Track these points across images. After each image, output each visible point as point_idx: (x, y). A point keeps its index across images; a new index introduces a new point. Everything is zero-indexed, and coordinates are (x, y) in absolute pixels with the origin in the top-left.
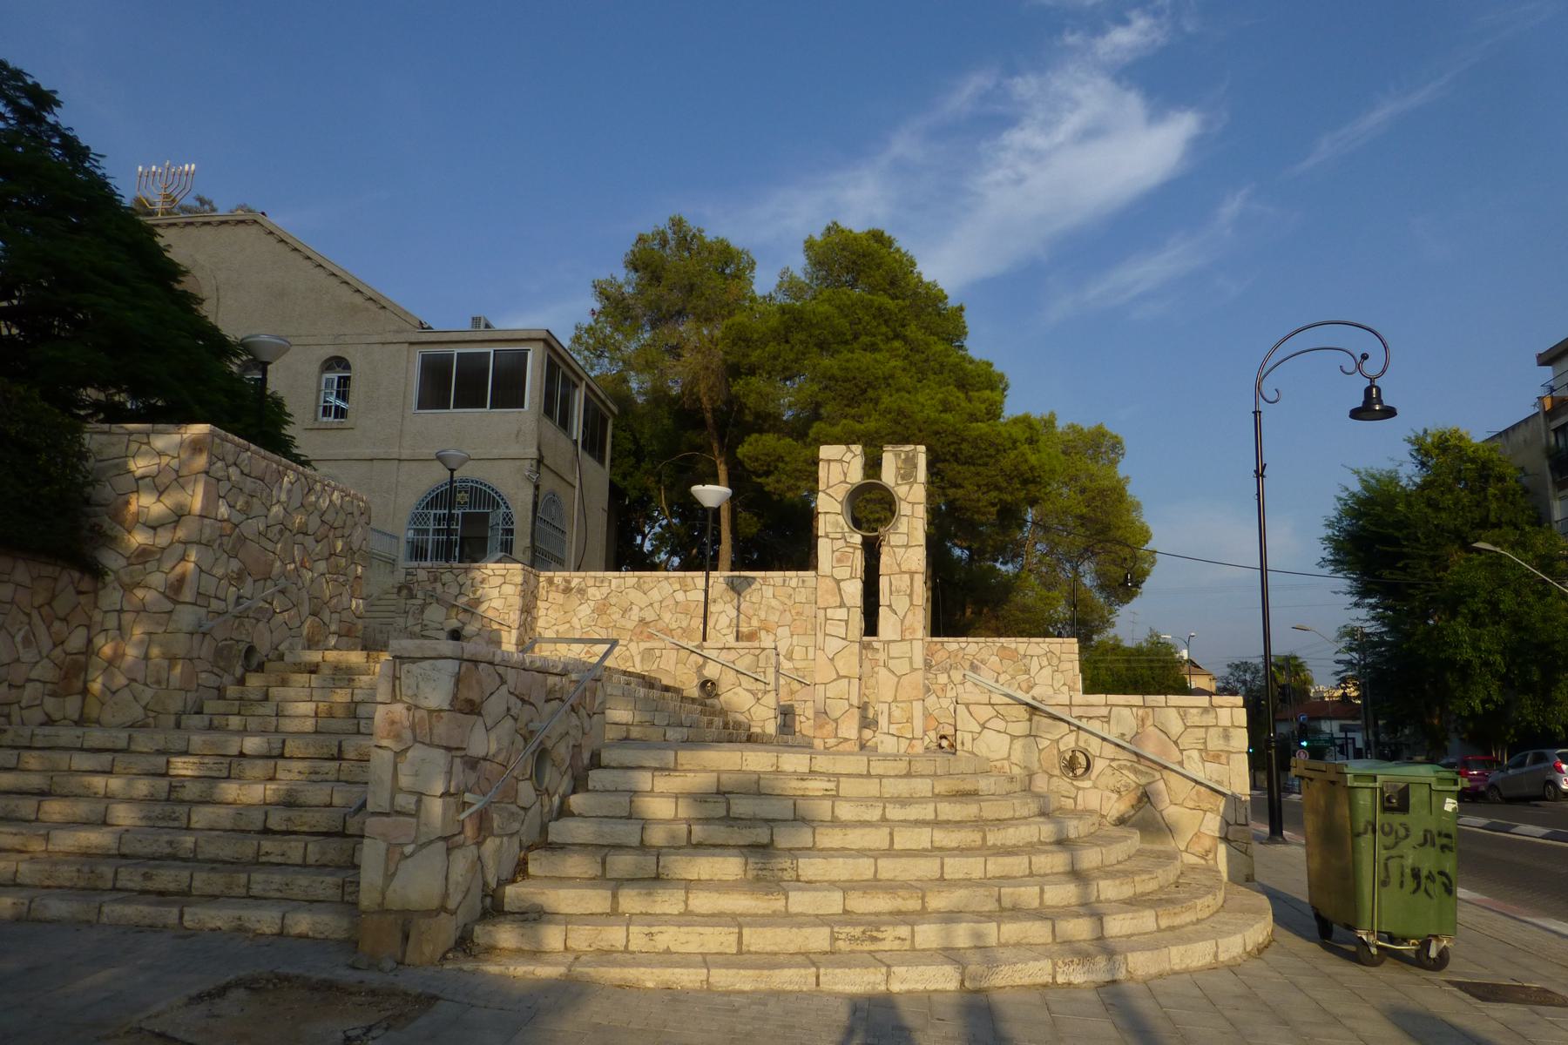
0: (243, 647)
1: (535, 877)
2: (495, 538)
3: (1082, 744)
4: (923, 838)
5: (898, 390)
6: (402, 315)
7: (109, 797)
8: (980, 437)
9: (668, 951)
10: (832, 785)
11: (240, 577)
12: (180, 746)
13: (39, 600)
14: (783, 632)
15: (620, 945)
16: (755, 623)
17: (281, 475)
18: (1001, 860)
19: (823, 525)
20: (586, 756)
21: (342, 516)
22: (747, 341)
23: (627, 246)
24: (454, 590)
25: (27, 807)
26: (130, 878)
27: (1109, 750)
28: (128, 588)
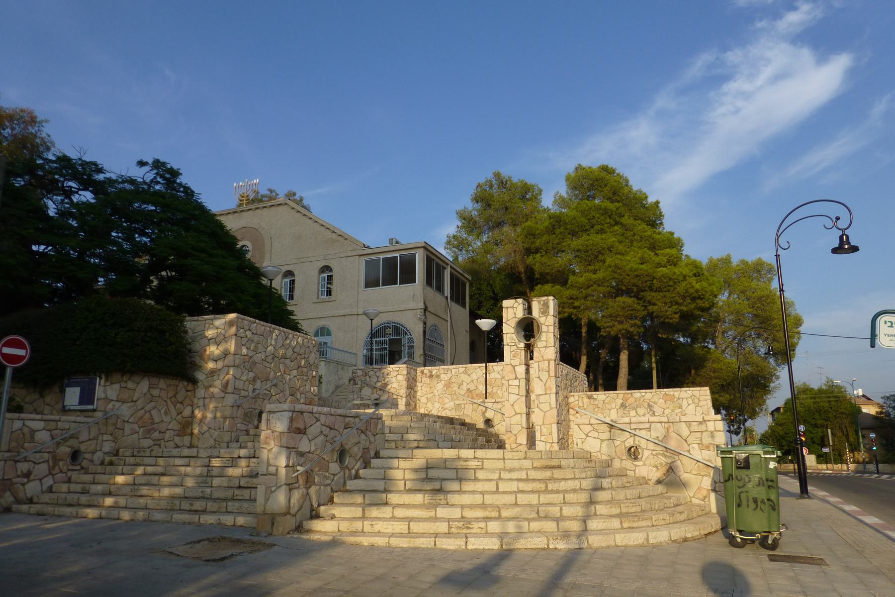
0: (257, 411)
1: (337, 504)
2: (405, 350)
3: (637, 443)
4: (513, 486)
5: (616, 254)
6: (355, 242)
7: (186, 475)
8: (663, 276)
9: (379, 532)
10: (480, 463)
11: (254, 380)
12: (216, 454)
13: (170, 395)
15: (360, 529)
17: (271, 333)
18: (547, 496)
19: (507, 339)
20: (372, 453)
21: (303, 348)
22: (533, 235)
23: (471, 191)
24: (375, 380)
25: (155, 479)
26: (185, 505)
27: (651, 446)
28: (207, 388)
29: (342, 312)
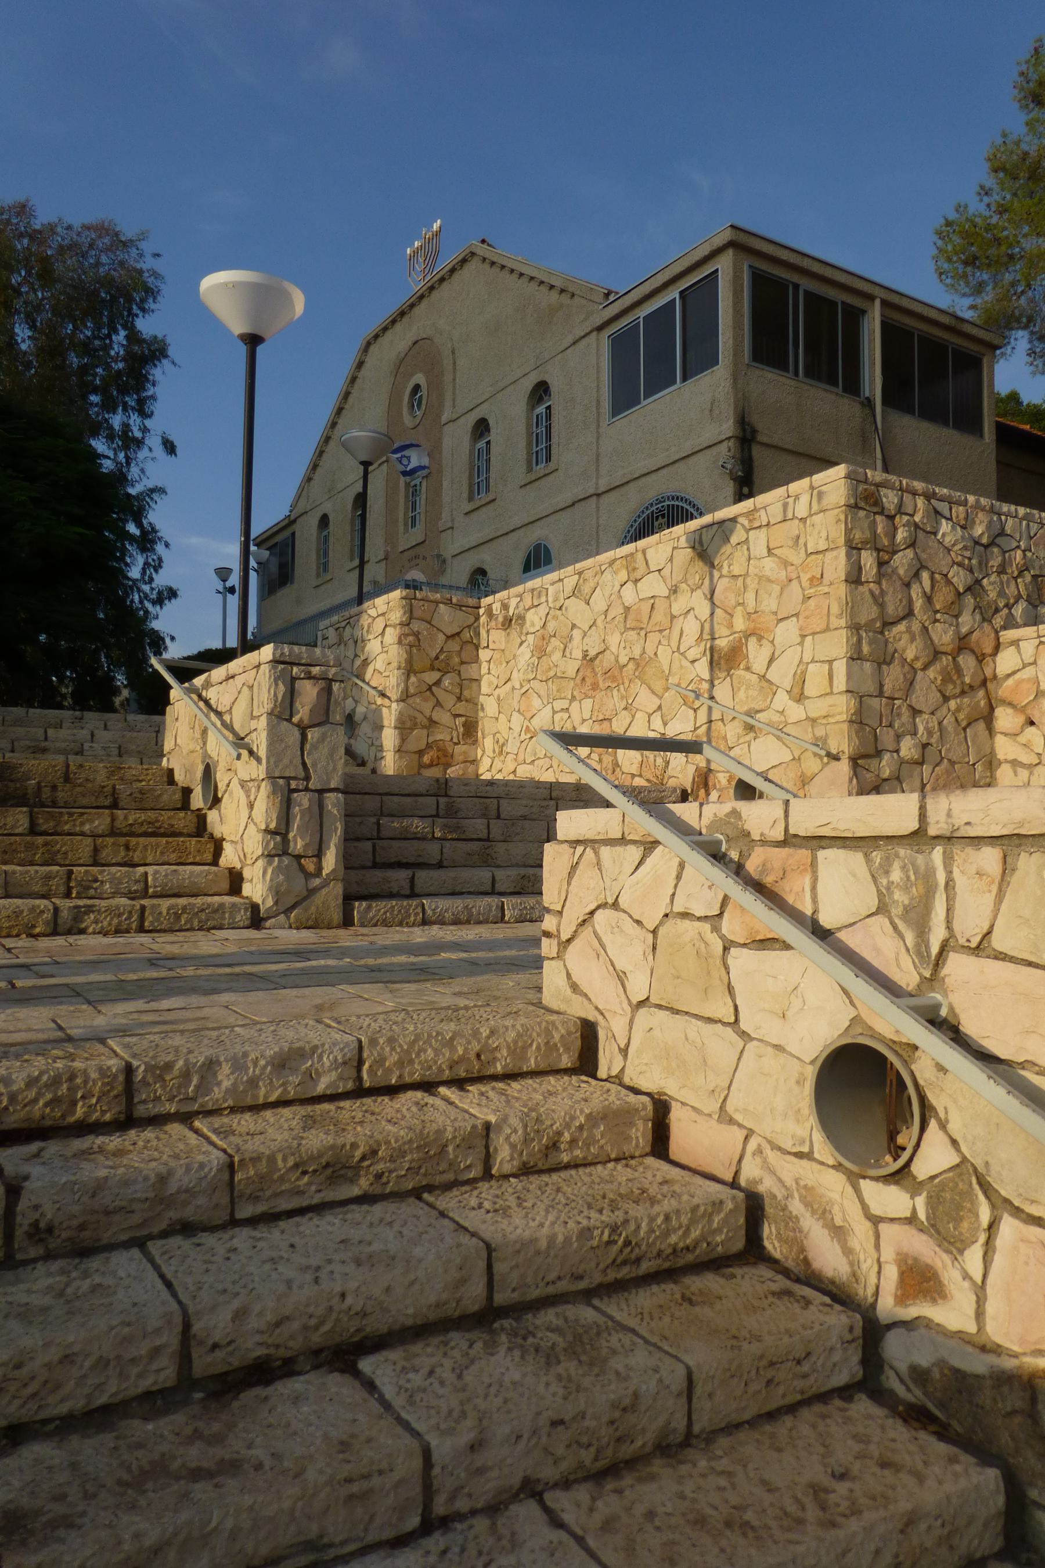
14: (786, 633)
16: (740, 623)
29: (567, 497)
